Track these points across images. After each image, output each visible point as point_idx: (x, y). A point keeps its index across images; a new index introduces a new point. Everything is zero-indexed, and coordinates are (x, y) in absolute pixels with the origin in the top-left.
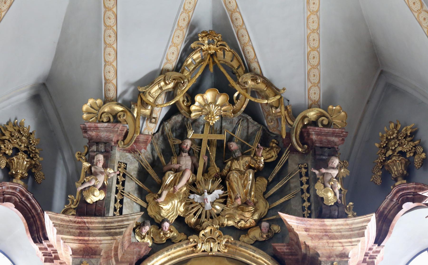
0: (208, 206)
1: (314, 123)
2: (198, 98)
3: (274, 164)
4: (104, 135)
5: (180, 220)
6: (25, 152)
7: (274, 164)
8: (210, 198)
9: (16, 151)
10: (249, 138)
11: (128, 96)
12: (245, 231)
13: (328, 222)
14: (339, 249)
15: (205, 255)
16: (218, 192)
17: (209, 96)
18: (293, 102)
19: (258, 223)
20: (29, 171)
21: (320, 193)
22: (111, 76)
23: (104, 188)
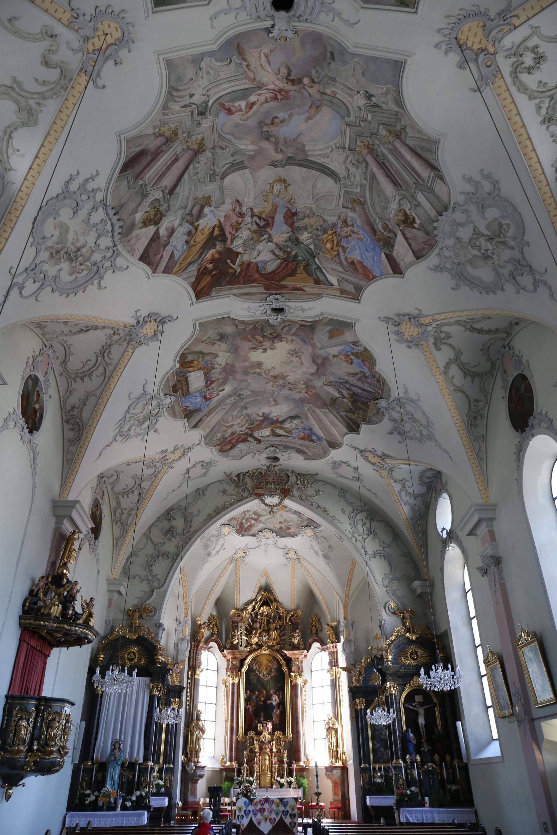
0: (264, 640)
1: (293, 616)
2: (262, 608)
3: (282, 626)
4: (236, 620)
5: (257, 643)
6: (216, 625)
7: (282, 626)
8: (264, 638)
9: (214, 625)
10: (275, 617)
11: (242, 607)
12: (274, 646)
13: (295, 651)
14: (297, 657)
15: (263, 654)
16: (267, 637)
17: (264, 607)
18: (287, 609)
19: (278, 644)
20: (218, 631)
21: (293, 641)
22: (238, 602)
23: (238, 639)
